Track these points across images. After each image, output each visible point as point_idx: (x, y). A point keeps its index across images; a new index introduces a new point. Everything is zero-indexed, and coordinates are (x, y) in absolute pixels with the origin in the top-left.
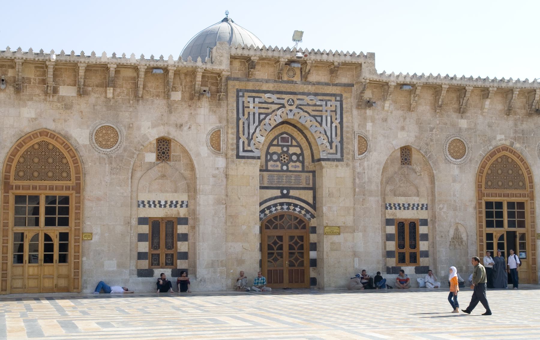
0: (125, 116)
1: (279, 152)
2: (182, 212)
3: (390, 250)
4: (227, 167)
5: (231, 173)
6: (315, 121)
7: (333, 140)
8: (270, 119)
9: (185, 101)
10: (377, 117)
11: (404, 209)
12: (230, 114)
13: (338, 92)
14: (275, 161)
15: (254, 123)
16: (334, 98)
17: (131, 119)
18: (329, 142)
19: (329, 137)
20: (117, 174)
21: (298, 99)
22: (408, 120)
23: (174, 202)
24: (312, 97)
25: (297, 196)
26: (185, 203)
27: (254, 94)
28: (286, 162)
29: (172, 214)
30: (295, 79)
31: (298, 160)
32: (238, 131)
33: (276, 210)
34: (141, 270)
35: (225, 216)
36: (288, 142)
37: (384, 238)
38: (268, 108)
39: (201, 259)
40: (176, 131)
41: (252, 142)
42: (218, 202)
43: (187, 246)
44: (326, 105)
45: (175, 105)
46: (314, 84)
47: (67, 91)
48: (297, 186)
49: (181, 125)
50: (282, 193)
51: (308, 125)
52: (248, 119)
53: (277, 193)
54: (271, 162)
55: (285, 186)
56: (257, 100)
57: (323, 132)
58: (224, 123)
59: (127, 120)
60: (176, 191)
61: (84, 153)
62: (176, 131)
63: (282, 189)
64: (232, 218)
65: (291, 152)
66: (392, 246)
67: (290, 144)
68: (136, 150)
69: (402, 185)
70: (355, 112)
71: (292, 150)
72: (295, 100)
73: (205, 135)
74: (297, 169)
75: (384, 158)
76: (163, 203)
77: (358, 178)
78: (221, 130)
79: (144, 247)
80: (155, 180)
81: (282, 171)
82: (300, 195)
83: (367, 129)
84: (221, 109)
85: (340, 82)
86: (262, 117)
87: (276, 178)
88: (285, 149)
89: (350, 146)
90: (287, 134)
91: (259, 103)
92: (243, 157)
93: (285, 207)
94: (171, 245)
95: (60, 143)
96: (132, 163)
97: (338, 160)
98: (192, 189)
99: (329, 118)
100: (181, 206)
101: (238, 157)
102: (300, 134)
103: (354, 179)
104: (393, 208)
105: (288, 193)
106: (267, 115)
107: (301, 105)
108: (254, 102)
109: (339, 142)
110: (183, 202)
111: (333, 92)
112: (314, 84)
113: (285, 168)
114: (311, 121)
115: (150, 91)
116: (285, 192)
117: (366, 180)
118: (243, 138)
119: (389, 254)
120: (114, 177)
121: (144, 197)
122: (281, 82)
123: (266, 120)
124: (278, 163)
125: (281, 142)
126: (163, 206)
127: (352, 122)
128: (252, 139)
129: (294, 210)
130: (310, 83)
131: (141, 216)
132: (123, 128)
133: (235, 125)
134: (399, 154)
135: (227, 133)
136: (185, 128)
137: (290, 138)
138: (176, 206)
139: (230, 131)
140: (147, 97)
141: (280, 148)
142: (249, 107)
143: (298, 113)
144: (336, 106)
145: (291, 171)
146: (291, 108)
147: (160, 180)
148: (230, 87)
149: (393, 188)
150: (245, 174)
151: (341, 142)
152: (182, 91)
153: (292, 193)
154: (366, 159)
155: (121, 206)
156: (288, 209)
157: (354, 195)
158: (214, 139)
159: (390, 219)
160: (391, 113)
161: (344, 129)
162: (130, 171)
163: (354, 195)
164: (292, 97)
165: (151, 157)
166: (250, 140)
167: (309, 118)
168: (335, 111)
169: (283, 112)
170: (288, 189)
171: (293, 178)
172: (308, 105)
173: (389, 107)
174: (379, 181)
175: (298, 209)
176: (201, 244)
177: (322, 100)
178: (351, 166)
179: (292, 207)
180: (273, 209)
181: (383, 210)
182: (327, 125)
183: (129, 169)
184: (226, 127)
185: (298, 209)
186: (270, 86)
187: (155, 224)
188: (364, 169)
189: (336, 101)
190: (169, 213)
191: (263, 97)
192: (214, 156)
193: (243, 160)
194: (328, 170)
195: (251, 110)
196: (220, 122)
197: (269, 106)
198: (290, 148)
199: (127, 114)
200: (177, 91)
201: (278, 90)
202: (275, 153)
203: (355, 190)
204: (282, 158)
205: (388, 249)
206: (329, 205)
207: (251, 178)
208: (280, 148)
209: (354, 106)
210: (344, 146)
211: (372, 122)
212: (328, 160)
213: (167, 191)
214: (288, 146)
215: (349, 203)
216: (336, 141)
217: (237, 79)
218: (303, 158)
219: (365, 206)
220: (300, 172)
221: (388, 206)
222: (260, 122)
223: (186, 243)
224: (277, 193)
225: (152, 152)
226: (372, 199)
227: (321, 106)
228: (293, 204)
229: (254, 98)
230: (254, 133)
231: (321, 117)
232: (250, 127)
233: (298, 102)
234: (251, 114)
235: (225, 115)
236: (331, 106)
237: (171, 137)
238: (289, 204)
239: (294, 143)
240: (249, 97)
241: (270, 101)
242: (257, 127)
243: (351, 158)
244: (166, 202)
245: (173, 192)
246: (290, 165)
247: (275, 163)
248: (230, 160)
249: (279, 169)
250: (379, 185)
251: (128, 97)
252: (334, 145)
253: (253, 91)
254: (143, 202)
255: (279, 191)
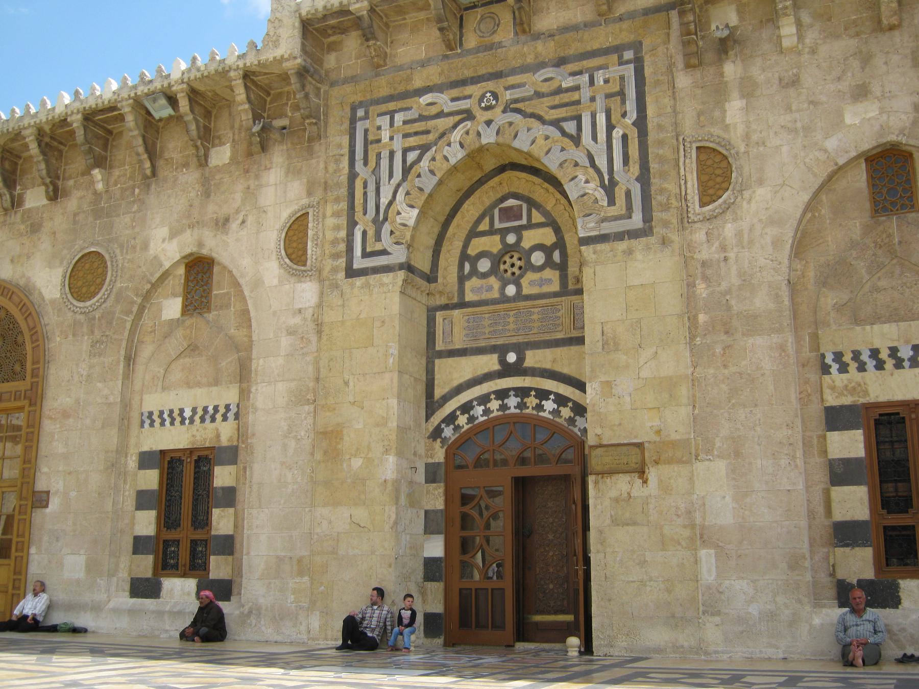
0: (123, 222)
1: (495, 250)
2: (226, 432)
3: (848, 518)
4: (320, 305)
5: (330, 316)
6: (556, 134)
7: (617, 177)
8: (433, 159)
9: (238, 163)
10: (761, 78)
11: (899, 364)
12: (332, 167)
13: (626, 37)
14: (484, 276)
15: (391, 176)
16: (615, 57)
17: (133, 227)
18: (603, 185)
19: (604, 169)
20: (100, 355)
21: (507, 89)
22: (879, 61)
23: (210, 409)
24: (549, 72)
25: (548, 366)
26: (234, 409)
27: (392, 106)
28: (517, 272)
29: (205, 440)
30: (497, 38)
31: (549, 263)
32: (352, 207)
33: (487, 412)
34: (138, 579)
35: (312, 435)
36: (520, 218)
37: (821, 477)
38: (427, 132)
39: (252, 553)
40: (215, 236)
41: (387, 228)
42: (298, 398)
43: (232, 519)
44: (592, 82)
45: (217, 177)
46: (551, 35)
47: (35, 199)
48: (547, 337)
49: (227, 220)
50: (502, 361)
51: (538, 150)
52: (376, 171)
53: (490, 363)
54: (474, 279)
55: (514, 340)
56: (399, 118)
57: (584, 161)
58: (319, 194)
59: (127, 232)
60: (216, 382)
61: (51, 320)
62: (215, 236)
63: (502, 350)
64: (329, 441)
65: (526, 244)
66: (855, 502)
67: (524, 221)
68: (137, 295)
69: (883, 283)
70: (683, 80)
71: (530, 238)
72: (500, 90)
73: (275, 232)
74: (546, 289)
75: (794, 201)
76: (188, 414)
77: (705, 278)
78: (311, 211)
79: (146, 523)
80: (178, 357)
81: (504, 299)
82: (554, 361)
83: (728, 120)
84: (314, 161)
85: (632, 8)
86: (412, 156)
87: (487, 322)
88: (511, 239)
89: (671, 186)
90: (516, 196)
91: (405, 122)
92: (364, 272)
93: (512, 401)
94: (202, 521)
95: (14, 304)
96: (128, 325)
97: (633, 234)
98: (244, 375)
99: (601, 119)
100: (225, 418)
101: (351, 273)
102: (551, 189)
103: (691, 285)
104: (853, 366)
105: (521, 359)
106: (424, 148)
107: (516, 101)
108: (392, 124)
109: (637, 179)
110: (227, 407)
111: (611, 41)
112: (551, 35)
113: (511, 290)
114: (547, 138)
115: (172, 159)
116: (512, 358)
117: (735, 281)
118: (364, 223)
119: (846, 534)
120: (95, 361)
121: (153, 402)
122: (459, 55)
123: (422, 164)
124: (493, 281)
125: (501, 220)
126: (187, 422)
127: (675, 112)
128: (386, 219)
129: (540, 407)
130: (537, 37)
131: (146, 448)
132: (118, 251)
133: (344, 191)
134: (859, 179)
135: (324, 217)
136: (234, 225)
137: (525, 206)
138: (213, 419)
139: (329, 212)
140: (166, 174)
141: (497, 238)
142: (379, 141)
143: (511, 124)
144: (622, 78)
145: (528, 298)
146: (488, 115)
147: (188, 360)
148: (333, 102)
149: (845, 297)
150: (363, 316)
151: (644, 178)
152: (234, 140)
153: (532, 359)
154: (729, 215)
155: (103, 427)
156: (522, 406)
157: (692, 338)
158: (295, 238)
159: (842, 407)
160: (813, 51)
161: (652, 137)
162: (124, 344)
163: (692, 338)
164: (490, 85)
165: (172, 308)
166: (378, 224)
167: (541, 131)
168: (622, 94)
169: (467, 133)
170: (520, 350)
171: (535, 317)
172: (539, 95)
173: (800, 37)
174: (781, 279)
175: (549, 405)
176: (254, 512)
177: (580, 73)
178: (676, 246)
179: (532, 401)
180: (479, 410)
181: (813, 376)
182: (595, 138)
183: (121, 340)
184: (322, 203)
185: (549, 405)
186: (432, 74)
187: (169, 463)
188: (723, 248)
189: (621, 63)
190: (198, 438)
191: (415, 106)
192: (293, 280)
193: (359, 281)
194: (598, 268)
195: (385, 146)
196: (310, 194)
197: (431, 124)
198: (525, 233)
199: (127, 219)
200: (224, 144)
201: (453, 77)
202: (482, 255)
203: (693, 320)
204: (507, 266)
205: (840, 514)
206: (603, 379)
207: (377, 324)
208: (497, 238)
209: (680, 65)
210: (653, 188)
211: (742, 96)
212: (603, 238)
213: (199, 385)
214: (518, 230)
215: (673, 362)
216: (627, 179)
217: (353, 79)
218: (564, 255)
219: (733, 369)
220: (555, 295)
221: (829, 359)
222: (407, 171)
223: (231, 511)
224: (490, 363)
225: (174, 295)
226: (760, 341)
227: (577, 88)
228: (536, 390)
229: (392, 114)
230: (390, 203)
231: (578, 119)
232: (382, 189)
233: (508, 95)
234: (385, 154)
235: (321, 174)
236: (606, 81)
237: (205, 252)
238: (523, 392)
239: (537, 217)
240: (379, 115)
241: (434, 110)
242: (398, 186)
243: (674, 221)
244: (194, 410)
245: (210, 385)
246: (524, 282)
247: (483, 282)
248: (327, 283)
249: (496, 294)
250: (785, 293)
251: (131, 183)
252: (620, 193)
253: (391, 98)
254: (151, 414)
255: (494, 358)
